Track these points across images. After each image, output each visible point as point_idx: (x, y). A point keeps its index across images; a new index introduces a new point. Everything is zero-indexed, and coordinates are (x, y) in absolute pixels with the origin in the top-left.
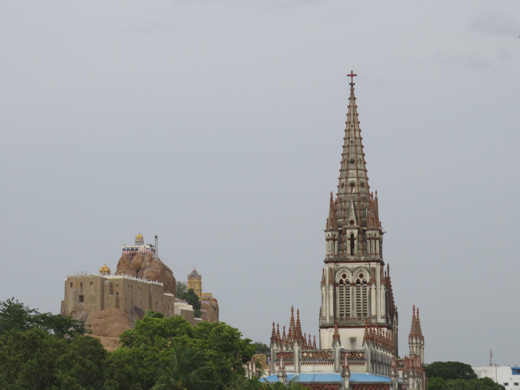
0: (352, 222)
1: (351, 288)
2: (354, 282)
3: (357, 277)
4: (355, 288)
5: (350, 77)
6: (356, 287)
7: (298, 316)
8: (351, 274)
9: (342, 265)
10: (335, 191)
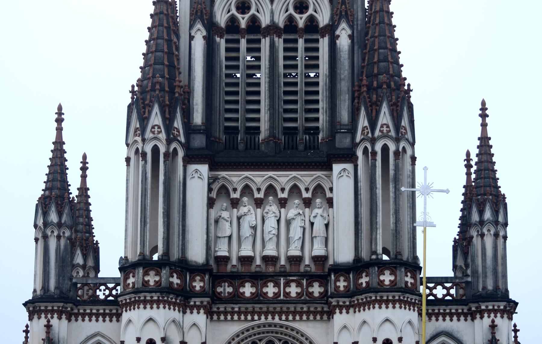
1: (265, 44)
2: (276, 19)
3: (287, 11)
4: (280, 43)
6: (281, 40)
7: (84, 177)
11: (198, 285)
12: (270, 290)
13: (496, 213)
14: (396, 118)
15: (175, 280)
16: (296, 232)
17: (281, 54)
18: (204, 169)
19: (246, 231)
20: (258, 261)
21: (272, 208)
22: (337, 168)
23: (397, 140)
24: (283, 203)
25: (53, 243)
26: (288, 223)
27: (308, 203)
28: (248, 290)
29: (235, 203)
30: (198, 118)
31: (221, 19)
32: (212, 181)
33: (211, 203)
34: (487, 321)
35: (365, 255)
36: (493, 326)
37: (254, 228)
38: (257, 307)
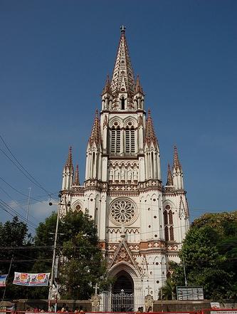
1: (121, 132)
11: (104, 186)
12: (123, 188)
17: (125, 134)
19: (117, 174)
21: (124, 169)
24: (126, 168)
29: (114, 168)
30: (105, 147)
34: (179, 196)
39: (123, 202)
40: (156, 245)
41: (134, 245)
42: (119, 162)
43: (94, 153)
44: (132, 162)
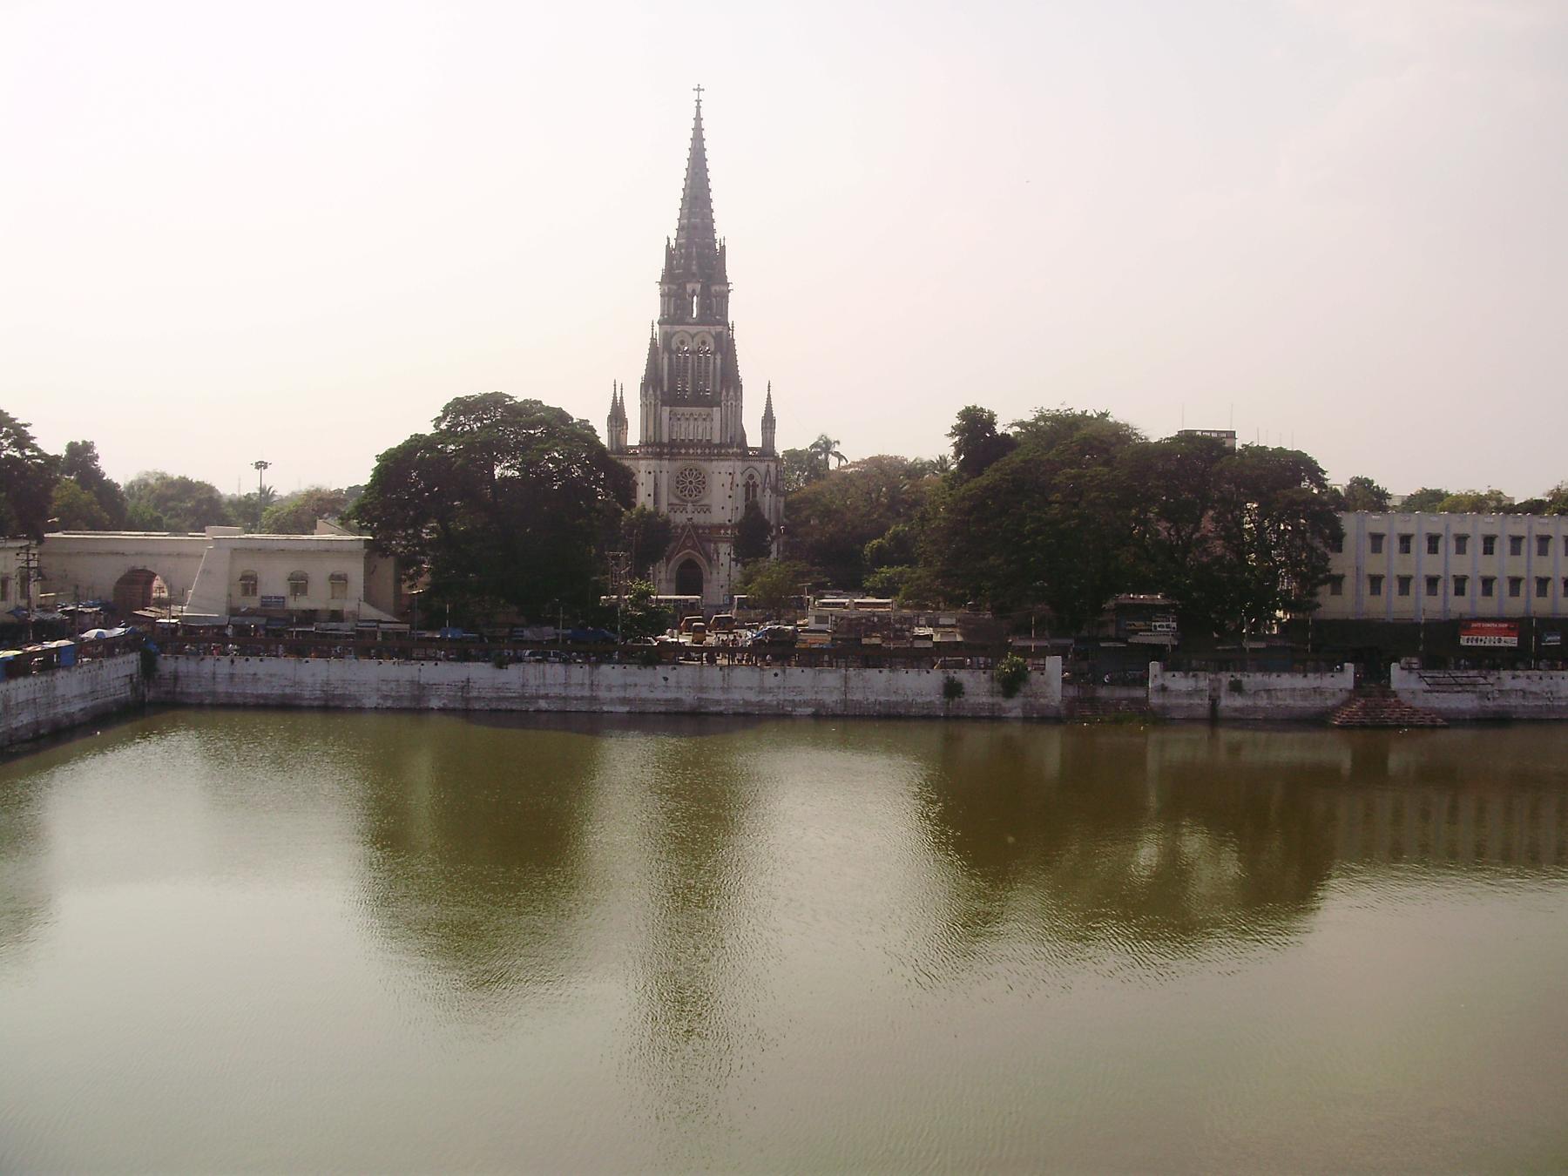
0: (694, 275)
5: (696, 92)
8: (691, 340)
9: (678, 328)
10: (673, 235)
11: (666, 451)
12: (691, 451)
13: (771, 424)
14: (736, 393)
15: (658, 450)
16: (700, 430)
18: (668, 409)
20: (687, 441)
22: (715, 409)
23: (736, 401)
25: (614, 432)
26: (698, 427)
27: (704, 419)
28: (683, 451)
30: (666, 389)
31: (674, 347)
32: (670, 412)
33: (670, 419)
35: (723, 442)
36: (768, 466)
37: (686, 429)
38: (687, 458)
39: (691, 470)
40: (729, 532)
41: (704, 528)
42: (687, 410)
43: (650, 403)
44: (703, 410)
